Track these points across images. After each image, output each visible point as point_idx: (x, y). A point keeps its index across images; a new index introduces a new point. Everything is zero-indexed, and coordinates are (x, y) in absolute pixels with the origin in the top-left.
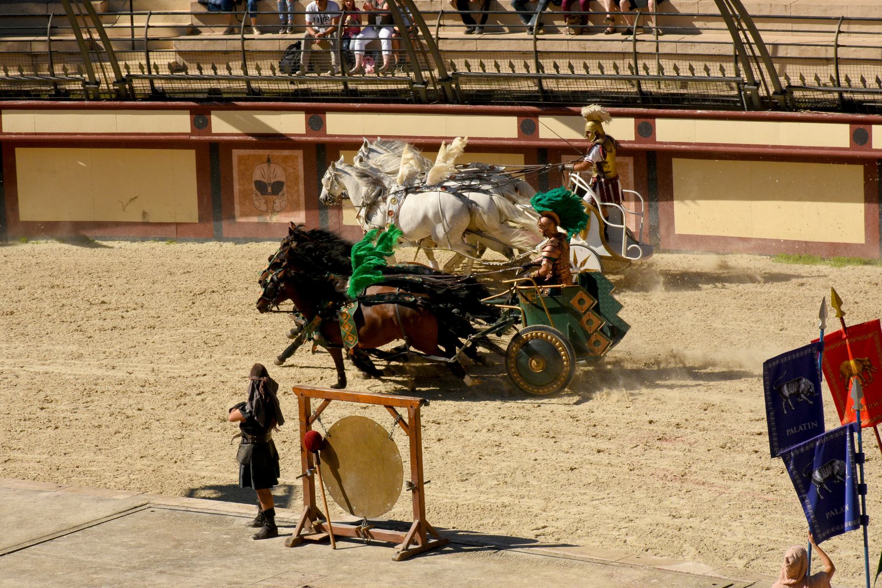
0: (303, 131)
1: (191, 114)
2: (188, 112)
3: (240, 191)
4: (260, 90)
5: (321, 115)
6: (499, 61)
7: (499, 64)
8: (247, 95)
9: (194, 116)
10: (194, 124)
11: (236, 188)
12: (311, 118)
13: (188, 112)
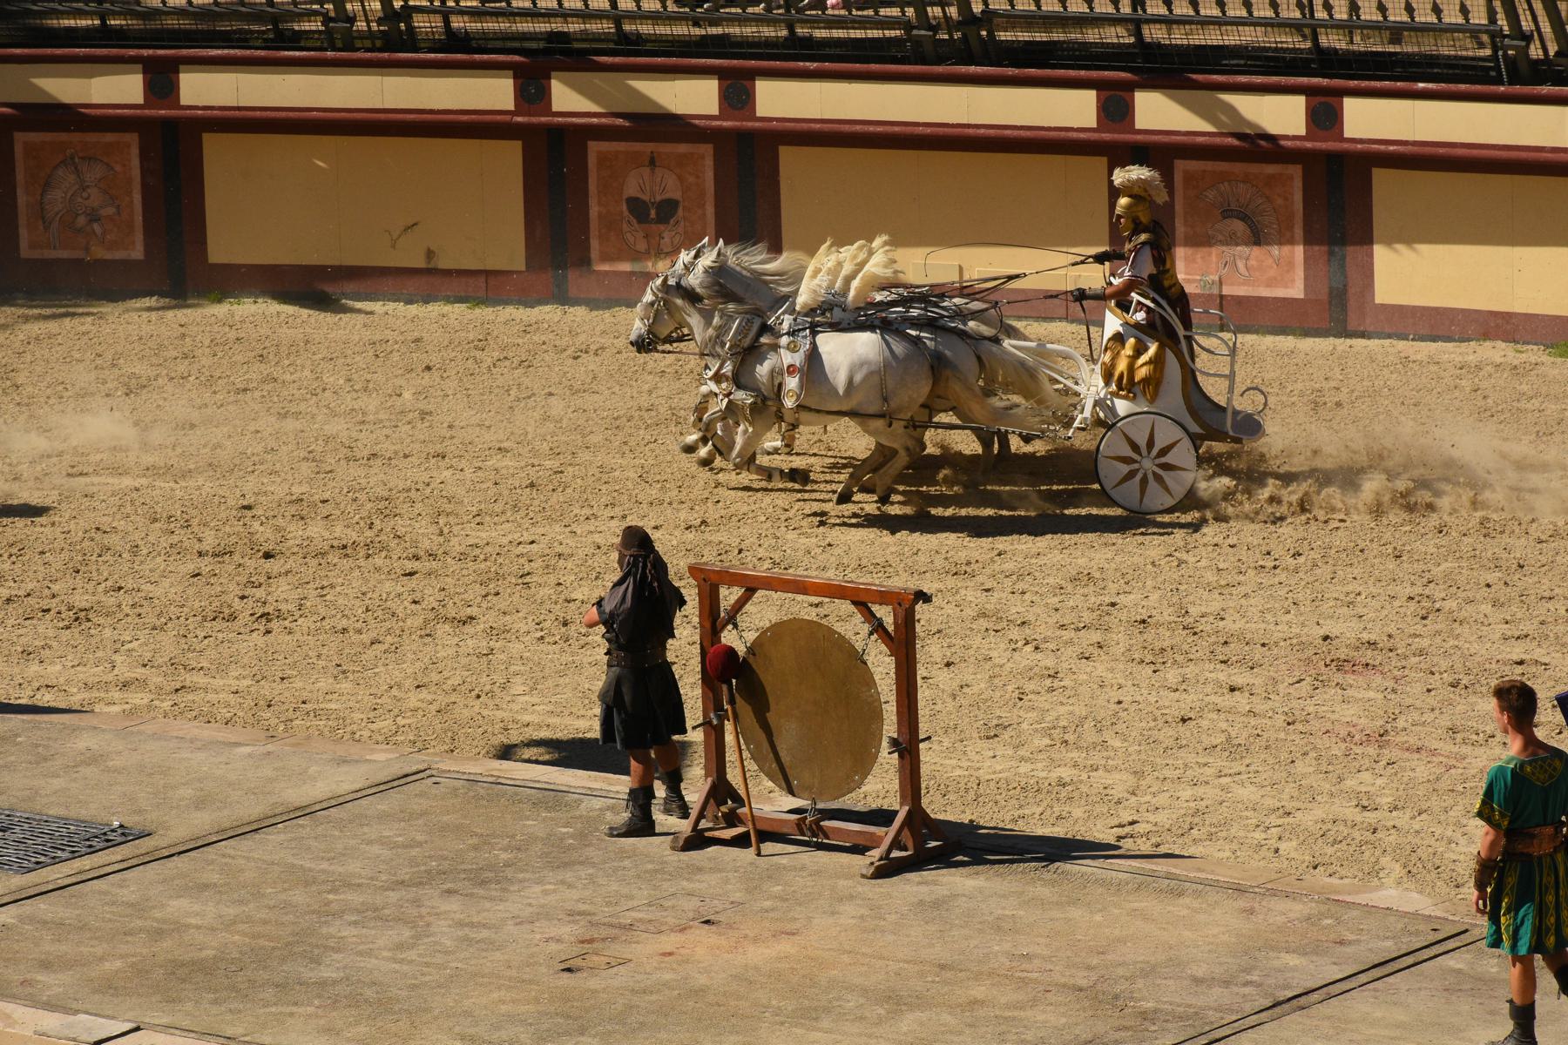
0: (715, 111)
1: (515, 77)
2: (511, 72)
3: (600, 216)
4: (639, 35)
5: (745, 83)
9: (520, 81)
10: (521, 94)
11: (594, 210)
12: (729, 87)
13: (511, 72)
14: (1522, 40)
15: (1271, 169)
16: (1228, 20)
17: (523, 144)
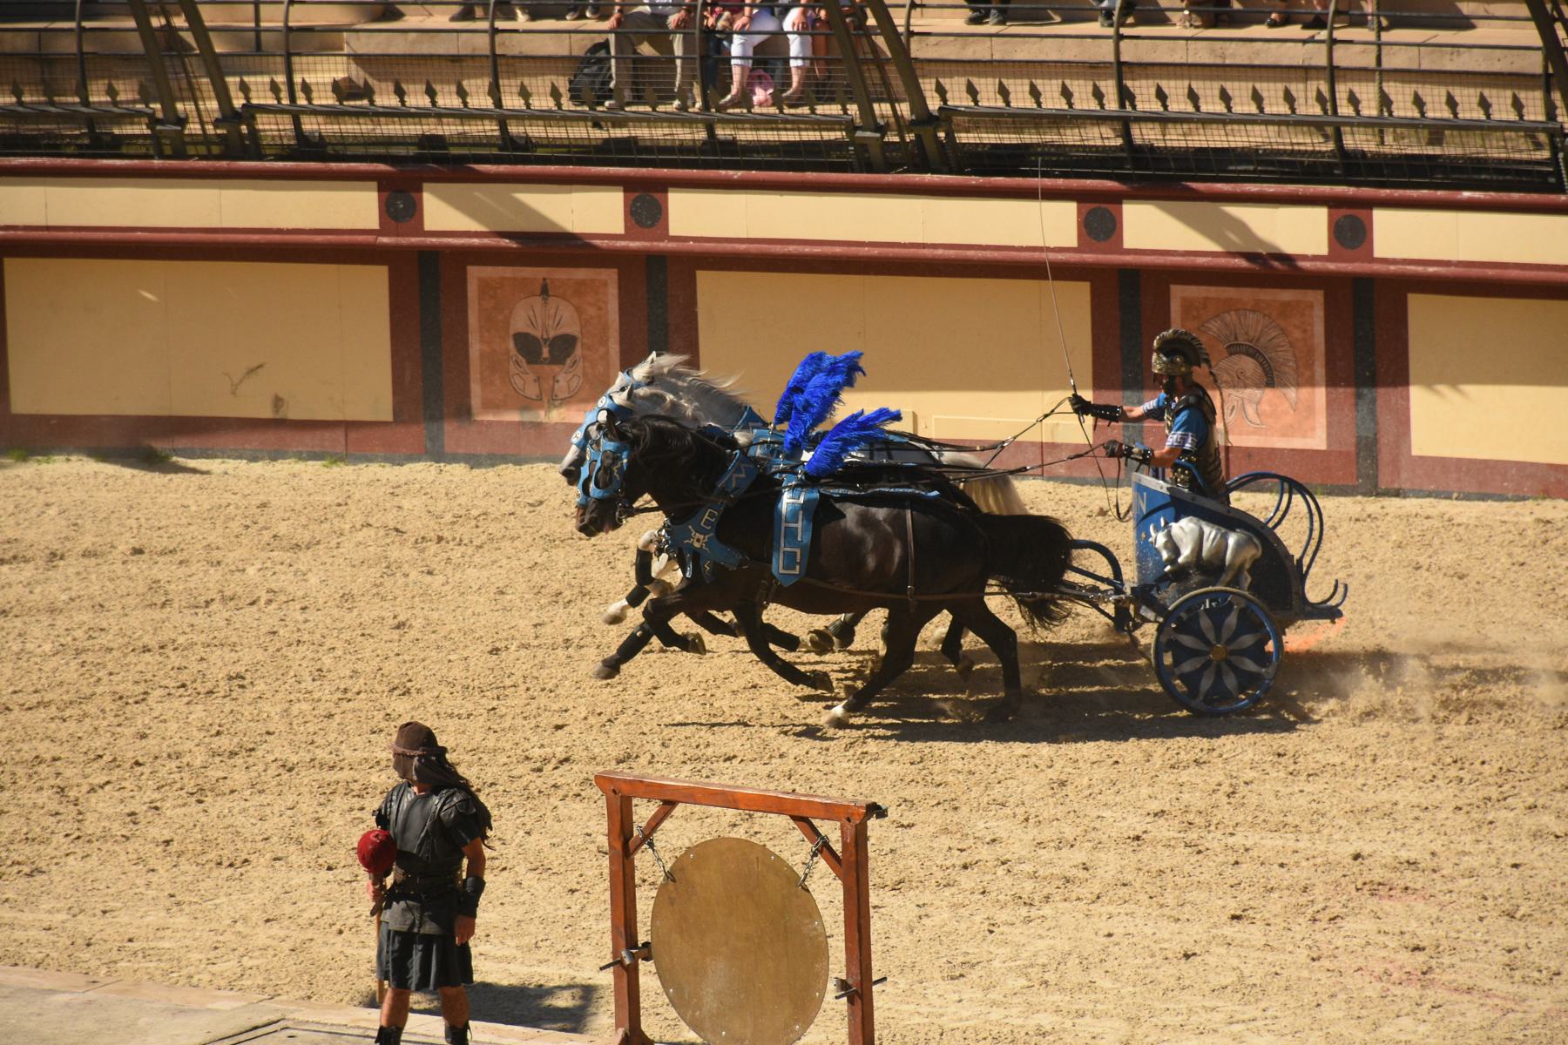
1: (380, 190)
2: (374, 184)
3: (482, 356)
4: (528, 139)
5: (657, 196)
6: (1039, 83)
7: (1040, 88)
8: (501, 150)
9: (386, 194)
11: (475, 348)
12: (635, 200)
14: (876, 131)
15: (1286, 295)
16: (981, 110)
17: (390, 270)
